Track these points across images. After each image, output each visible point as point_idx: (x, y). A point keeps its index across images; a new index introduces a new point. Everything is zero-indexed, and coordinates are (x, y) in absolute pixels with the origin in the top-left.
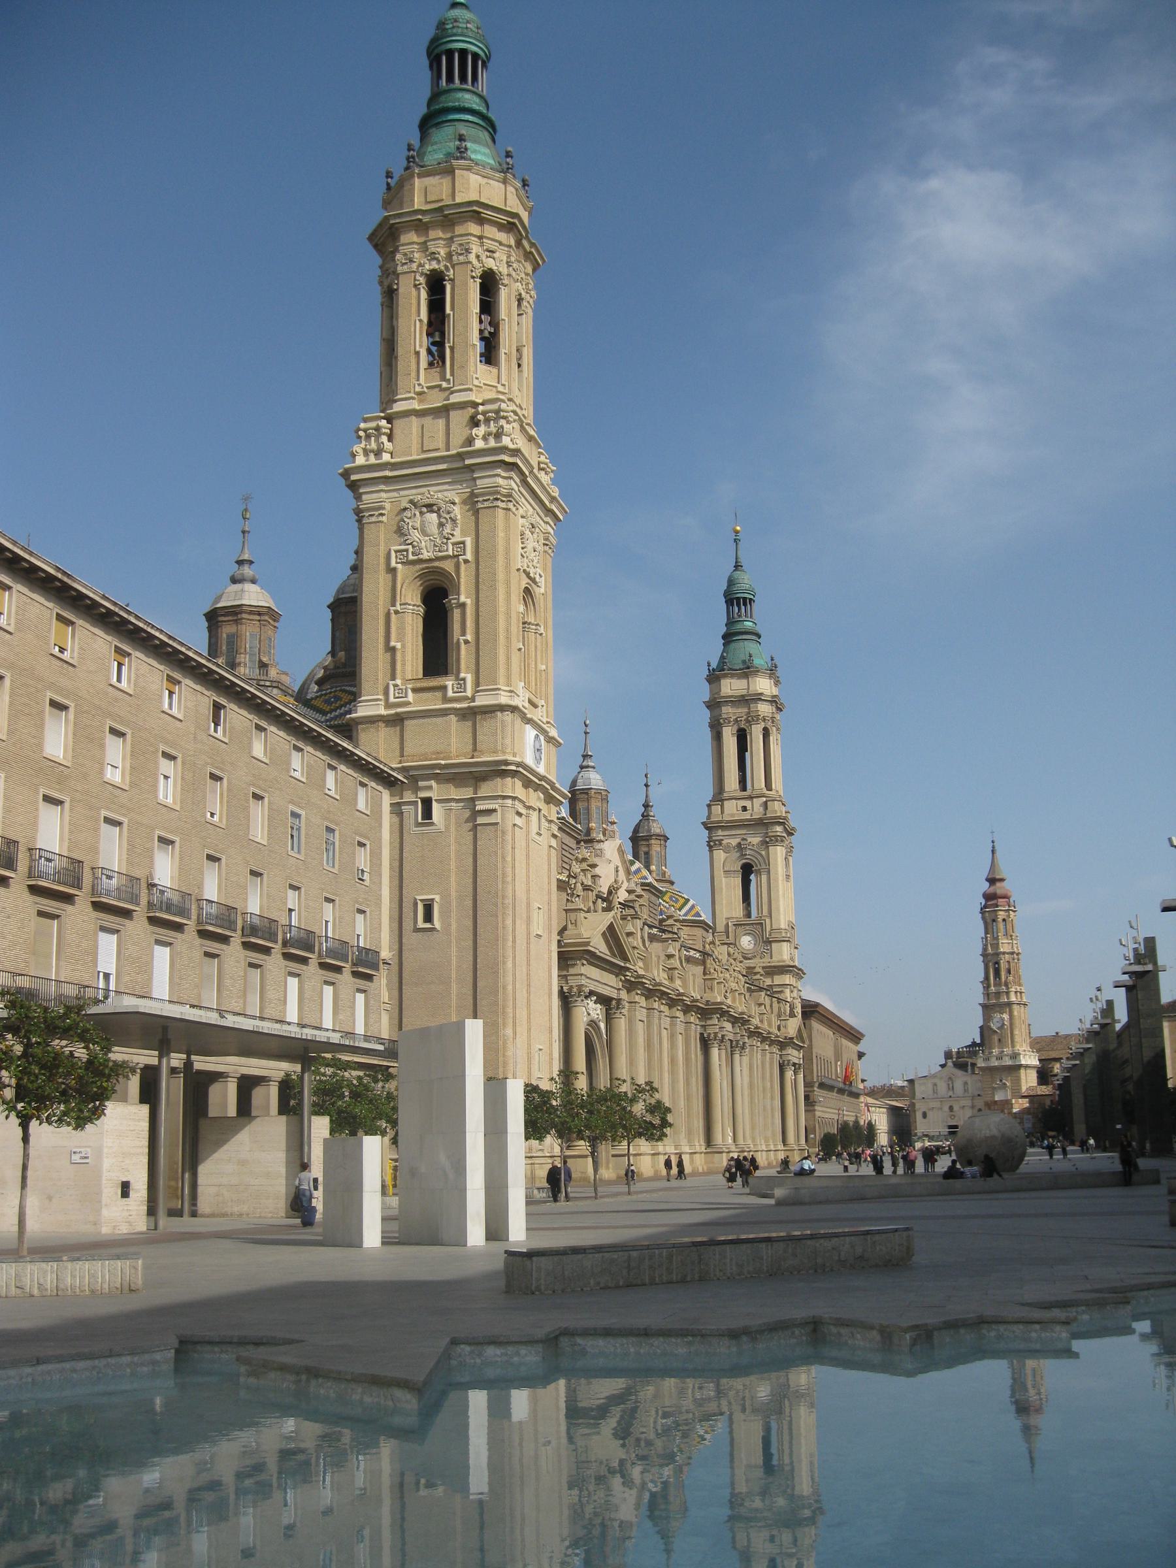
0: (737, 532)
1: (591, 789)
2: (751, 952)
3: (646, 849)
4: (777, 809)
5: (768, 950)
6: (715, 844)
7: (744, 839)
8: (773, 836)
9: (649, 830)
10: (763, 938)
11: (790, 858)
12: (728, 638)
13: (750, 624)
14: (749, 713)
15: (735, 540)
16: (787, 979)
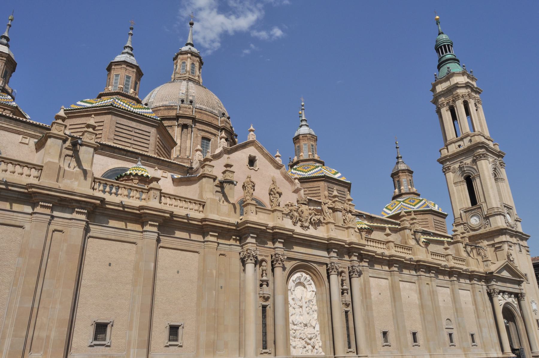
0: (437, 20)
1: (299, 135)
2: (478, 225)
3: (397, 179)
4: (478, 139)
5: (488, 222)
6: (447, 170)
7: (461, 163)
8: (477, 155)
9: (398, 168)
10: (483, 216)
11: (503, 171)
12: (439, 67)
13: (450, 56)
14: (453, 96)
15: (437, 24)
16: (503, 238)
